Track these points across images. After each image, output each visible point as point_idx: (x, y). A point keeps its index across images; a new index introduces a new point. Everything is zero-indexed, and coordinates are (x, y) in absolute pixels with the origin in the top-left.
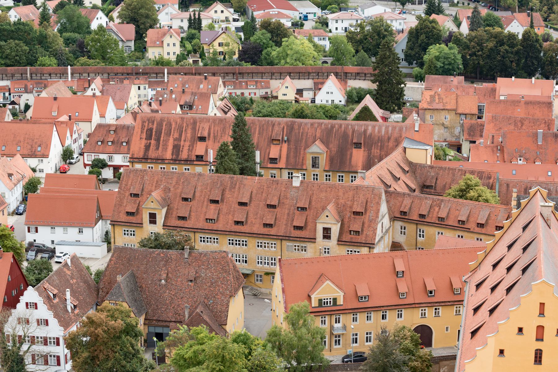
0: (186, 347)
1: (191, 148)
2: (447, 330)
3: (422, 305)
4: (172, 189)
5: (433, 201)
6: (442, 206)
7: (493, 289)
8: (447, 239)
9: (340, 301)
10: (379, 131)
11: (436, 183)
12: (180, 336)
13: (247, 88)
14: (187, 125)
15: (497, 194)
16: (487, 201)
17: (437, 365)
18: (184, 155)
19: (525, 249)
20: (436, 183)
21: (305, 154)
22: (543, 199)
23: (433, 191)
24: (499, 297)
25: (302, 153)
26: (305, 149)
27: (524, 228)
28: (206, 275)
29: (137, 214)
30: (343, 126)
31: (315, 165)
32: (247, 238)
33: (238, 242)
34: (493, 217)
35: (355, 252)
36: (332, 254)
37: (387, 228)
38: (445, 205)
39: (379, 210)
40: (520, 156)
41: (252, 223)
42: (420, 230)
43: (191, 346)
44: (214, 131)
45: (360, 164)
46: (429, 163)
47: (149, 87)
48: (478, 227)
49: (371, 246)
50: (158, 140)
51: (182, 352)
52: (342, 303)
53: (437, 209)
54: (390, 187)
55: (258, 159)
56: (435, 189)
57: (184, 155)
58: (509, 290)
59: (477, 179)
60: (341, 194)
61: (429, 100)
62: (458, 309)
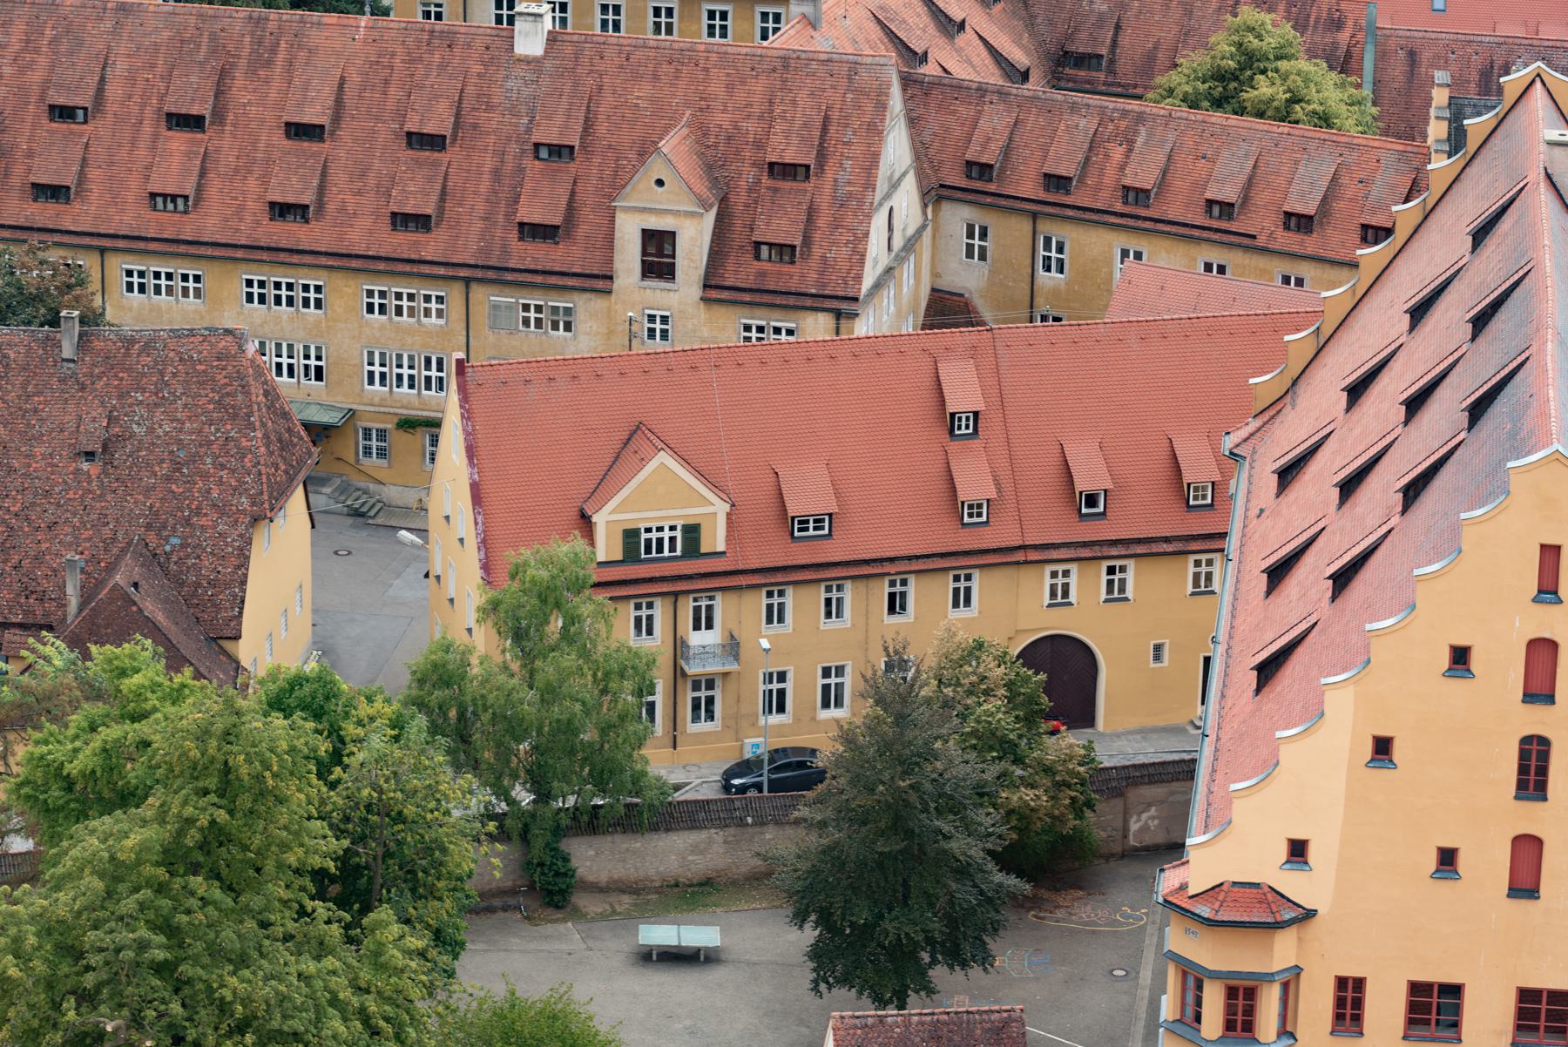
0: (71, 732)
2: (1157, 658)
3: (1054, 555)
5: (1104, 117)
6: (1140, 140)
7: (1349, 487)
8: (1157, 280)
9: (716, 539)
11: (1114, 43)
12: (47, 684)
15: (1367, 91)
16: (1324, 120)
17: (1118, 803)
19: (1480, 322)
20: (1114, 43)
22: (1556, 115)
23: (1102, 76)
24: (1372, 522)
27: (1480, 235)
28: (151, 430)
32: (324, 273)
33: (284, 293)
34: (1350, 188)
35: (777, 331)
36: (679, 342)
37: (910, 231)
38: (1150, 135)
39: (874, 158)
41: (342, 209)
42: (1048, 241)
43: (93, 729)
48: (1287, 227)
49: (842, 307)
51: (58, 752)
52: (721, 547)
53: (1118, 153)
54: (924, 58)
56: (1111, 71)
58: (1413, 491)
59: (1287, 29)
60: (717, 88)
62: (1204, 569)
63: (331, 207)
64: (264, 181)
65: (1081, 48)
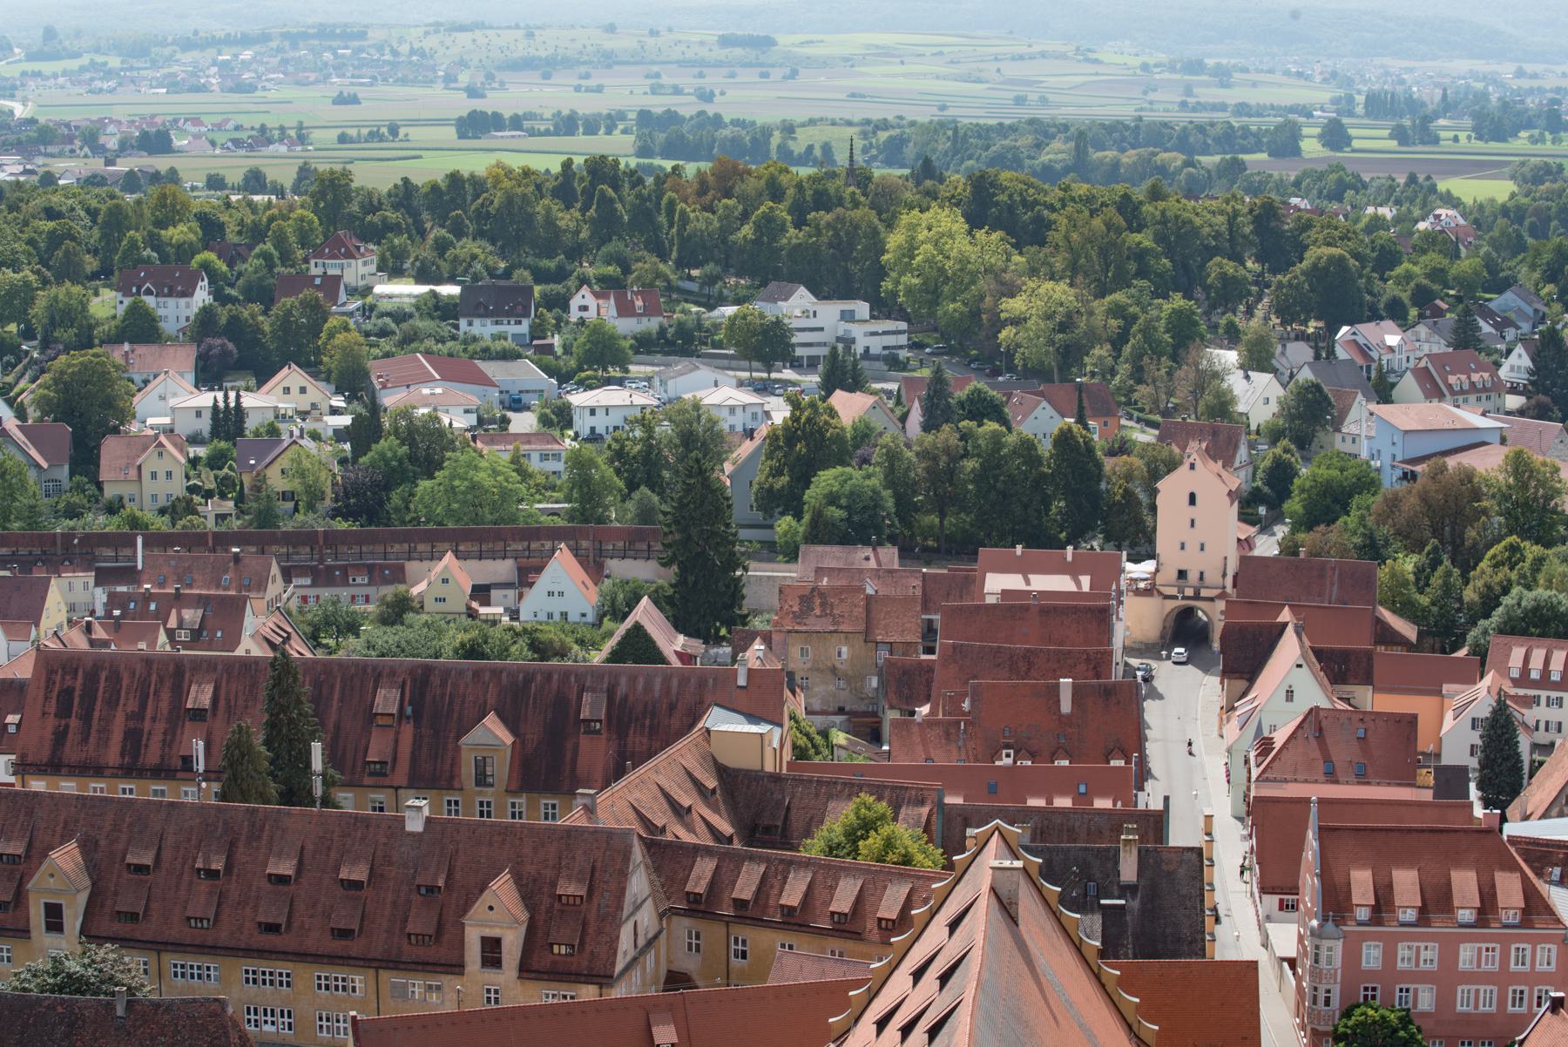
1: (171, 737)
4: (102, 843)
10: (648, 688)
11: (786, 818)
13: (346, 584)
14: (161, 679)
18: (152, 756)
19: (944, 979)
20: (786, 818)
21: (458, 749)
25: (450, 747)
26: (458, 738)
27: (953, 926)
29: (16, 907)
30: (556, 677)
31: (482, 780)
32: (290, 965)
33: (268, 977)
35: (565, 997)
36: (505, 1004)
37: (650, 935)
39: (622, 891)
40: (1008, 746)
41: (302, 926)
42: (736, 940)
44: (228, 693)
45: (598, 775)
46: (769, 767)
47: (97, 584)
49: (604, 979)
50: (87, 718)
54: (663, 830)
55: (317, 763)
57: (152, 756)
61: (796, 609)
63: (295, 925)
64: (256, 908)
65: (766, 821)
